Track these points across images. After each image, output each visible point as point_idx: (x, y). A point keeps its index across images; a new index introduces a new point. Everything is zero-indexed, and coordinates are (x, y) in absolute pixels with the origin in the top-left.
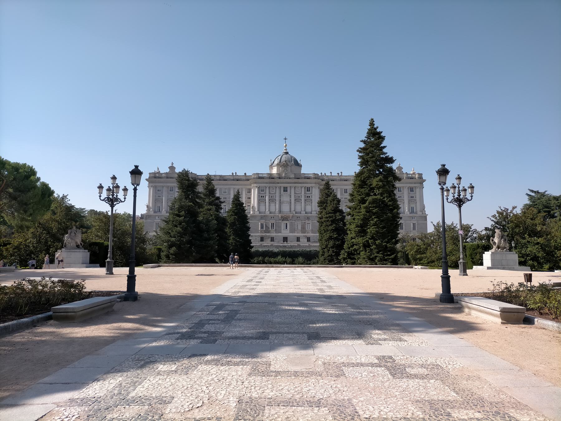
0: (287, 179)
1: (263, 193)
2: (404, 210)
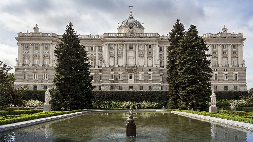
0: (132, 37)
2: (228, 64)
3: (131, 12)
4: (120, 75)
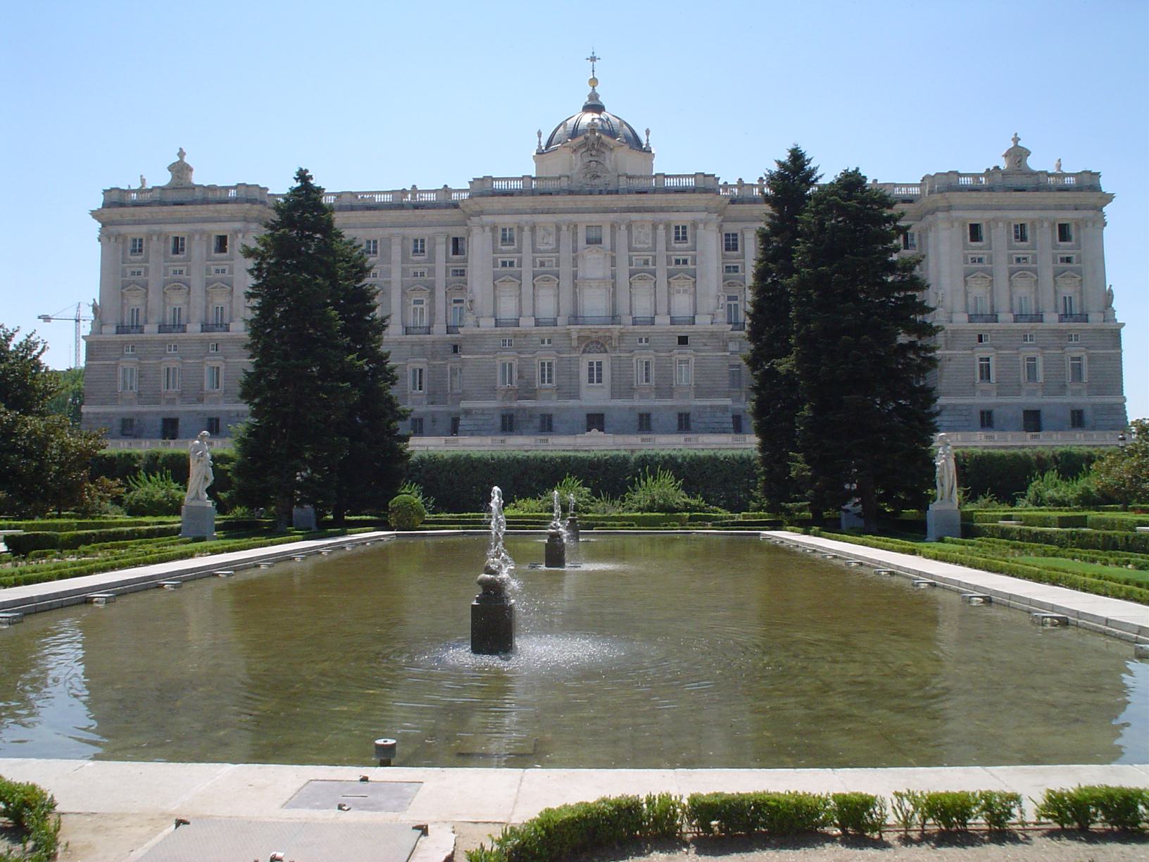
0: (600, 193)
1: (509, 252)
3: (594, 82)
4: (543, 364)
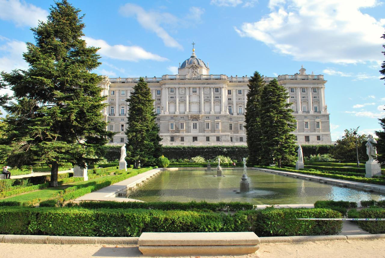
0: (196, 79)
1: (172, 94)
4: (181, 124)
